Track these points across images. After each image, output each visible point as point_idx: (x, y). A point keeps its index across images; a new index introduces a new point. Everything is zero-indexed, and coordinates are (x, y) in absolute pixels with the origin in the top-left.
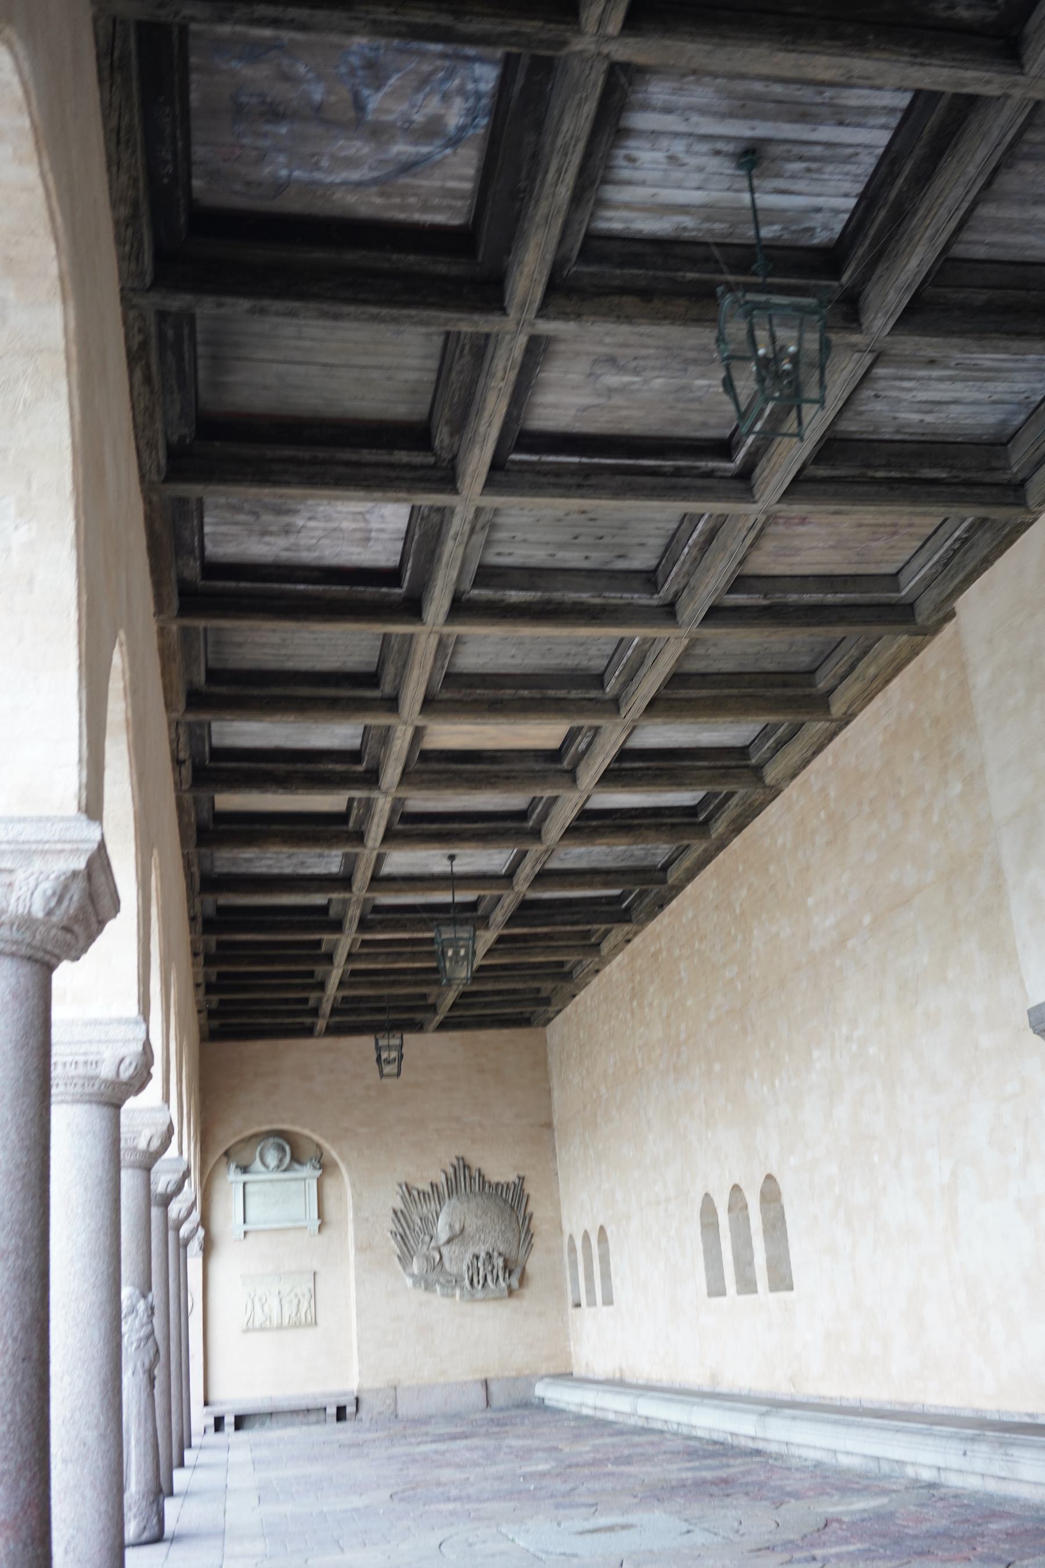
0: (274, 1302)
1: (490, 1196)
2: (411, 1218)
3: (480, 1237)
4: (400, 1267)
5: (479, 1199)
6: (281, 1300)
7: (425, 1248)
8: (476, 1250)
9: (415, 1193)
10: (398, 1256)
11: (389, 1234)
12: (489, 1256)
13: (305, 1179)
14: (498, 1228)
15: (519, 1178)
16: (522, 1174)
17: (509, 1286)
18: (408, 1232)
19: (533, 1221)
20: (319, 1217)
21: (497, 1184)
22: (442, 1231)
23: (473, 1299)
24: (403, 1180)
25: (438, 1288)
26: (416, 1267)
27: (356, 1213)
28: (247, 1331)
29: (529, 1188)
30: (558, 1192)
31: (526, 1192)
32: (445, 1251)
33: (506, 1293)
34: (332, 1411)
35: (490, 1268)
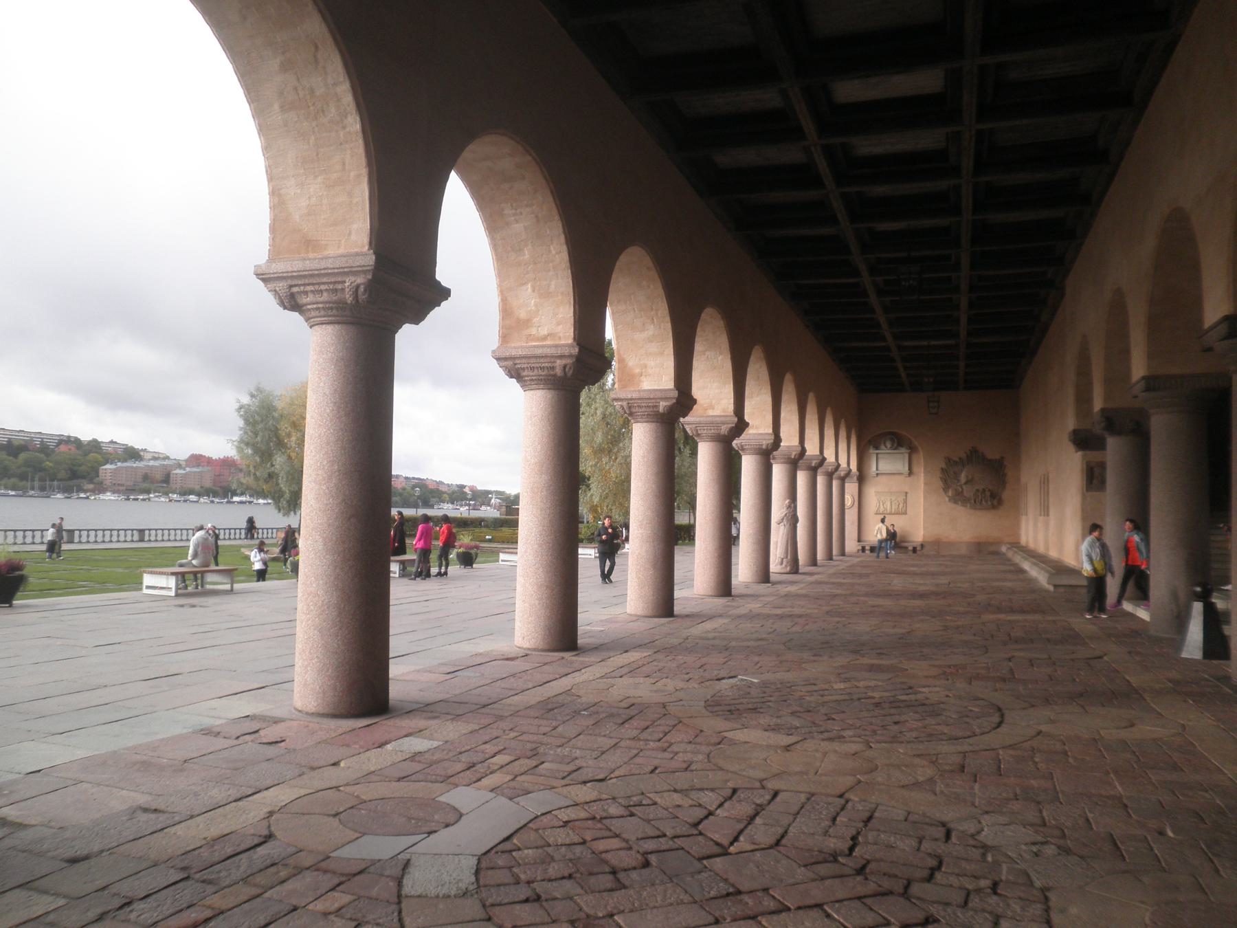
0: (888, 504)
12: (984, 490)
17: (992, 504)
22: (963, 478)
25: (960, 503)
28: (876, 514)
32: (964, 487)
34: (910, 548)
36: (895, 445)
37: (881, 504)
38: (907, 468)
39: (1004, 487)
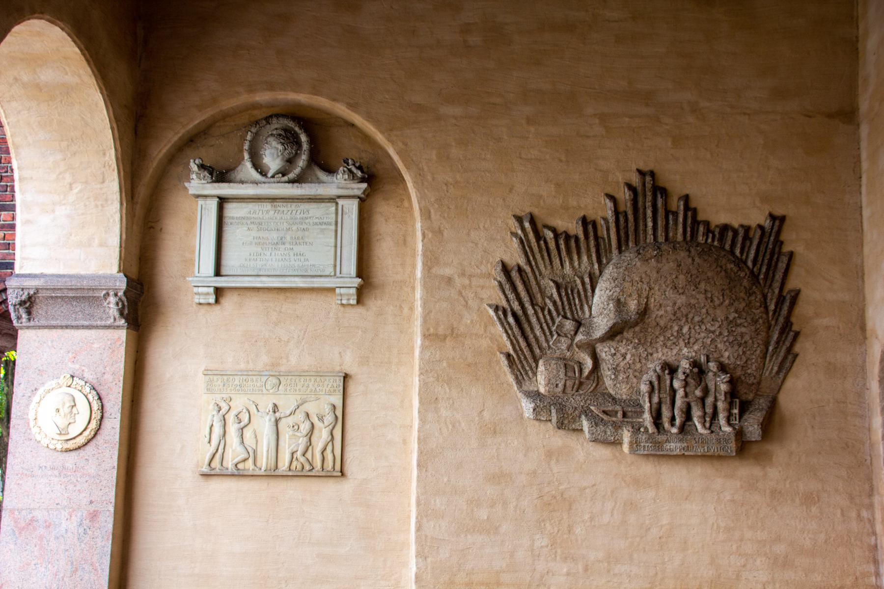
0: (264, 426)
1: (706, 251)
2: (538, 284)
3: (681, 328)
4: (511, 379)
5: (683, 254)
6: (277, 422)
7: (564, 343)
8: (670, 356)
9: (549, 235)
10: (508, 356)
11: (491, 312)
12: (699, 371)
13: (333, 200)
14: (720, 314)
15: (772, 217)
16: (779, 211)
17: (740, 434)
18: (530, 311)
19: (797, 310)
20: (359, 275)
21: (725, 228)
23: (659, 455)
24: (524, 209)
25: (585, 424)
26: (541, 382)
27: (428, 268)
29: (793, 240)
30: (860, 253)
31: (786, 249)
32: (604, 351)
33: (733, 445)
35: (698, 393)
36: (302, 161)
37: (233, 429)
38: (350, 265)
39: (789, 358)
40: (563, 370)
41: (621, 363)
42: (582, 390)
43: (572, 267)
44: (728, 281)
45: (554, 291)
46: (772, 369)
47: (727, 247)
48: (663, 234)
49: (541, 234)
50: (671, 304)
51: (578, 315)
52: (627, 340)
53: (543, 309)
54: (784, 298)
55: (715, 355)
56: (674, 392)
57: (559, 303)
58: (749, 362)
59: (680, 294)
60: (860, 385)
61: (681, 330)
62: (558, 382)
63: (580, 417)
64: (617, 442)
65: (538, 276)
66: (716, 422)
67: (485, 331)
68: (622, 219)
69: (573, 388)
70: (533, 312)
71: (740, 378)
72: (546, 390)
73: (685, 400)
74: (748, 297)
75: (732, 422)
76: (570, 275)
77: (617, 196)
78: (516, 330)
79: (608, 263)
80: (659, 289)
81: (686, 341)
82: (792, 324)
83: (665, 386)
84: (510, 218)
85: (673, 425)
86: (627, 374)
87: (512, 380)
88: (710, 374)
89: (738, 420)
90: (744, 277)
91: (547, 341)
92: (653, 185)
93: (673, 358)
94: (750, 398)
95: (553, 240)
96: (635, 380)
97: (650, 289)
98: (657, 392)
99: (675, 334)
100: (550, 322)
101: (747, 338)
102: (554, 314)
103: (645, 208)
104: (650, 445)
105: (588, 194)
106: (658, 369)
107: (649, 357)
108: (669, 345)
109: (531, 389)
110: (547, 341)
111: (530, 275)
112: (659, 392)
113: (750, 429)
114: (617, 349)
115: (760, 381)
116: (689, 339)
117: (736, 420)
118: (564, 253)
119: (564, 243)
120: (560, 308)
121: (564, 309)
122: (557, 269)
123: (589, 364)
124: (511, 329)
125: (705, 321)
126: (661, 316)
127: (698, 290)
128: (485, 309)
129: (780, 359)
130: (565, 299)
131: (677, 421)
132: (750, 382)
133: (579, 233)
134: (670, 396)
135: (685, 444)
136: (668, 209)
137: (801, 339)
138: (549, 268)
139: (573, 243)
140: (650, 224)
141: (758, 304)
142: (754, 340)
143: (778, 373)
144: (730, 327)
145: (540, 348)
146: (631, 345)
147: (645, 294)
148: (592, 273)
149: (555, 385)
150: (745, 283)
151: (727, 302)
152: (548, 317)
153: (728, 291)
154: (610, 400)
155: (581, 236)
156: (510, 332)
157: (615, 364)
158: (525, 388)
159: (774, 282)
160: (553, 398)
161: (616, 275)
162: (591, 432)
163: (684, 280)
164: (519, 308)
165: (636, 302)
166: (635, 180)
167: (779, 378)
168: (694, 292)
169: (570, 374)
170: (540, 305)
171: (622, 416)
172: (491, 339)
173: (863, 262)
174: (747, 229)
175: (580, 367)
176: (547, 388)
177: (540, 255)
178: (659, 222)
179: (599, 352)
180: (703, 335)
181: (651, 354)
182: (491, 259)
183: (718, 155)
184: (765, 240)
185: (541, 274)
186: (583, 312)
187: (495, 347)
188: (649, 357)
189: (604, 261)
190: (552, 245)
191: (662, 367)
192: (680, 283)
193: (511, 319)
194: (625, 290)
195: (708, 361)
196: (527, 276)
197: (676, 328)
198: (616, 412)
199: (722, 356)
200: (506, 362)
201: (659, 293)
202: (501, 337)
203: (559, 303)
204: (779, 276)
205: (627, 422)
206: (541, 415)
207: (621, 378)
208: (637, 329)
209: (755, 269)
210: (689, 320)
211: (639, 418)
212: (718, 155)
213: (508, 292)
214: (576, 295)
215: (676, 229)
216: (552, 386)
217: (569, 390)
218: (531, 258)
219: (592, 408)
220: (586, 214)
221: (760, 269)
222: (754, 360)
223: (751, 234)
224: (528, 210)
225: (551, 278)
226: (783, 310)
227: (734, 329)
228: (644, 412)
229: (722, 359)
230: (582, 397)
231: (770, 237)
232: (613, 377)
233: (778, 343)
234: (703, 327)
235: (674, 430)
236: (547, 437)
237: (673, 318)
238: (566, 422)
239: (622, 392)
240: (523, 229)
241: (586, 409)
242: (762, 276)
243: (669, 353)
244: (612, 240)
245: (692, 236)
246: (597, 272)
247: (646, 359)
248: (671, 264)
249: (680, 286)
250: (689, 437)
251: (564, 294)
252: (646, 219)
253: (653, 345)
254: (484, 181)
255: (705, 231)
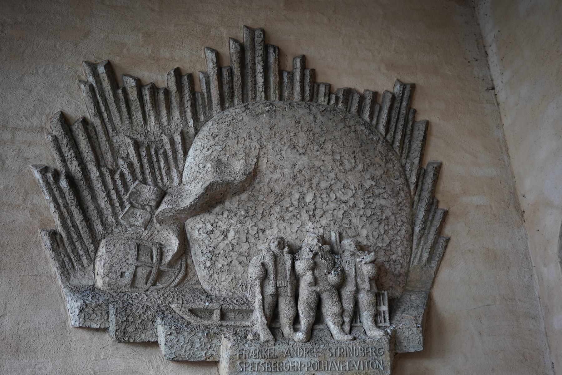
2: (109, 140)
4: (54, 268)
5: (302, 111)
9: (130, 83)
10: (53, 235)
11: (37, 175)
14: (353, 180)
16: (408, 79)
21: (349, 93)
31: (421, 117)
40: (133, 252)
41: (221, 244)
42: (162, 284)
43: (160, 124)
44: (359, 143)
45: (132, 151)
46: (421, 255)
47: (354, 109)
48: (277, 92)
49: (121, 85)
50: (289, 166)
51: (163, 182)
52: (230, 211)
53: (112, 173)
54: (425, 171)
55: (350, 233)
56: (296, 278)
57: (137, 165)
58: (393, 245)
59: (300, 154)
60: (527, 277)
61: (303, 198)
62: (124, 270)
63: (153, 321)
64: (211, 359)
65: (111, 131)
66: (358, 324)
67: (25, 200)
68: (225, 73)
69: (147, 279)
70: (98, 174)
71: (383, 265)
72: (104, 283)
73: (314, 288)
74: (385, 164)
75: (380, 325)
76: (155, 133)
77: (220, 50)
78: (70, 197)
79: (206, 121)
80: (273, 148)
81: (311, 213)
82: (438, 202)
83: (285, 269)
84: (81, 65)
85: (296, 330)
86: (230, 260)
87: (56, 269)
88: (347, 254)
89: (388, 321)
90: (378, 142)
91: (115, 214)
92: (264, 40)
93: (294, 237)
94: (397, 294)
95: (135, 89)
96: (240, 268)
97: (262, 147)
98: (272, 277)
99: (296, 203)
100: (121, 188)
101: (388, 213)
102: (129, 177)
103: (255, 64)
104: (263, 361)
105: (184, 47)
106: (273, 247)
107: (261, 234)
108: (287, 218)
109: (84, 282)
110: (115, 214)
111: (99, 129)
112: (276, 278)
113: (407, 334)
114: (214, 225)
115: (408, 271)
116: (314, 210)
117: (385, 322)
118: (148, 105)
119: (150, 92)
120: (138, 171)
121: (143, 173)
122: (138, 125)
123: (174, 244)
124: (64, 197)
125: (334, 188)
126: (276, 181)
127: (324, 150)
128: (29, 171)
129: (430, 242)
130: (145, 160)
131: (302, 323)
132: (396, 272)
133: (170, 85)
134: (291, 284)
135: (316, 359)
136: (282, 68)
137: (451, 219)
138: (127, 122)
139: (162, 96)
140: (260, 80)
141: (397, 174)
142: (398, 216)
143: (429, 260)
144: (366, 197)
145: (104, 223)
146: (235, 219)
147: (254, 153)
148: (185, 132)
149: (119, 274)
150: (380, 147)
151: (360, 167)
152: (119, 182)
153: (360, 154)
154: (203, 297)
155: (173, 88)
156: (60, 201)
157: (212, 245)
158: (74, 281)
159: (412, 152)
160: (115, 294)
161: (217, 131)
162: (170, 344)
163: (305, 138)
164: (78, 169)
165: (242, 161)
166: (243, 36)
167: (431, 267)
168: (318, 153)
169: (144, 258)
170: (110, 167)
171: (219, 318)
172: (32, 211)
173: (504, 136)
174: (375, 94)
175: (161, 249)
176: (107, 279)
177: (115, 106)
178: (272, 79)
179: (190, 230)
180: (332, 205)
181: (263, 231)
182: (48, 110)
183: (336, 21)
184: (397, 105)
185: (114, 129)
186: (170, 178)
187: (36, 223)
188: (261, 234)
189: (202, 118)
190: (133, 95)
191: (279, 243)
192: (300, 141)
193: (64, 184)
194: (228, 148)
195: (341, 238)
196: (95, 131)
197: (297, 196)
198: (211, 312)
199: (358, 234)
200: (48, 243)
201: (274, 153)
202: (47, 208)
203: (137, 165)
204: (416, 145)
205: (227, 326)
206: (91, 320)
207: (220, 266)
208: (244, 196)
209: (388, 137)
210: (314, 186)
211: (246, 321)
212: (336, 21)
213: (65, 149)
214: (161, 157)
215: (292, 89)
216: (114, 276)
217: (141, 282)
218: (103, 109)
219: (173, 306)
220: (181, 67)
221: (394, 137)
222: (398, 243)
223: (380, 100)
224: (106, 58)
225: (128, 134)
226: (426, 184)
227: (371, 200)
228: (252, 311)
229: (360, 239)
230: (161, 293)
231: (401, 103)
232: (208, 264)
233: (425, 222)
234: (333, 196)
235: (300, 336)
236: (102, 357)
237: (292, 183)
238: (130, 330)
239: (221, 287)
240: (95, 74)
241: (164, 309)
242: (397, 144)
243: (288, 229)
244: (212, 95)
245: (311, 100)
246: (192, 131)
247: (256, 236)
248: (287, 120)
249: (300, 145)
250: (322, 346)
251: (144, 154)
252: (255, 76)
253: (266, 218)
254: (53, 24)
255: (327, 92)
